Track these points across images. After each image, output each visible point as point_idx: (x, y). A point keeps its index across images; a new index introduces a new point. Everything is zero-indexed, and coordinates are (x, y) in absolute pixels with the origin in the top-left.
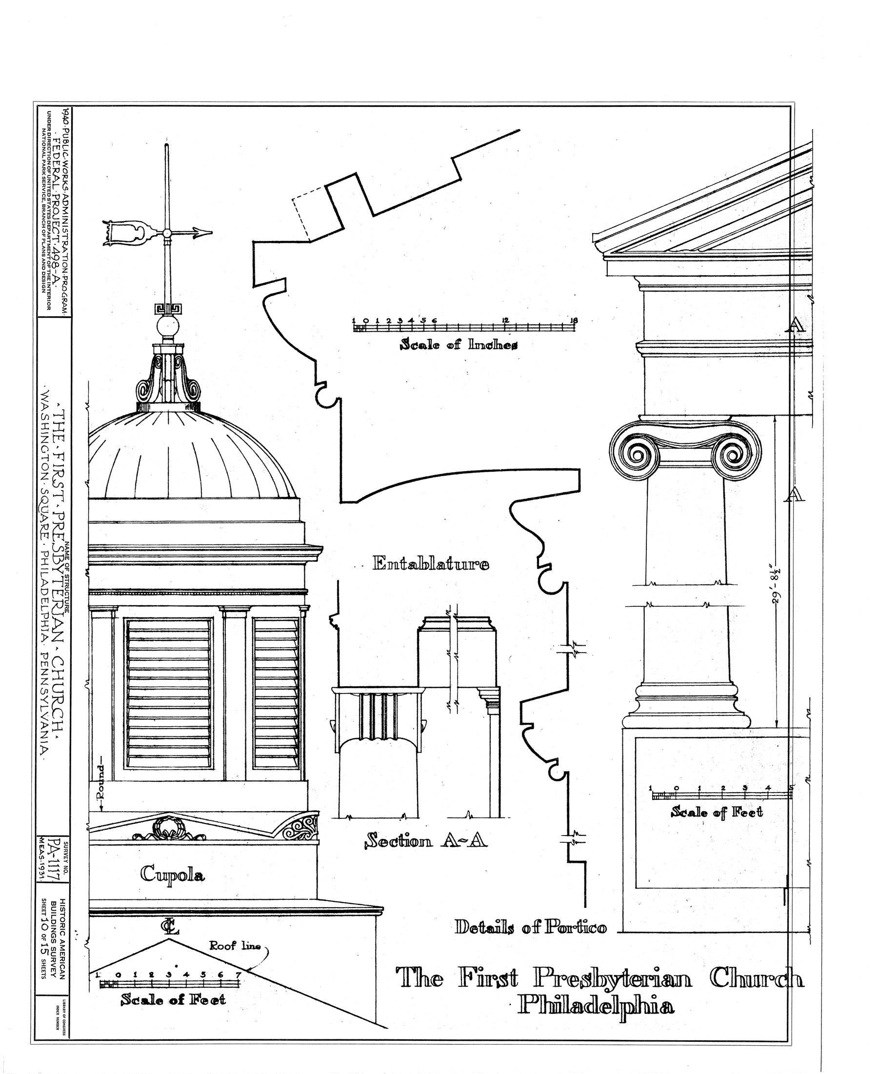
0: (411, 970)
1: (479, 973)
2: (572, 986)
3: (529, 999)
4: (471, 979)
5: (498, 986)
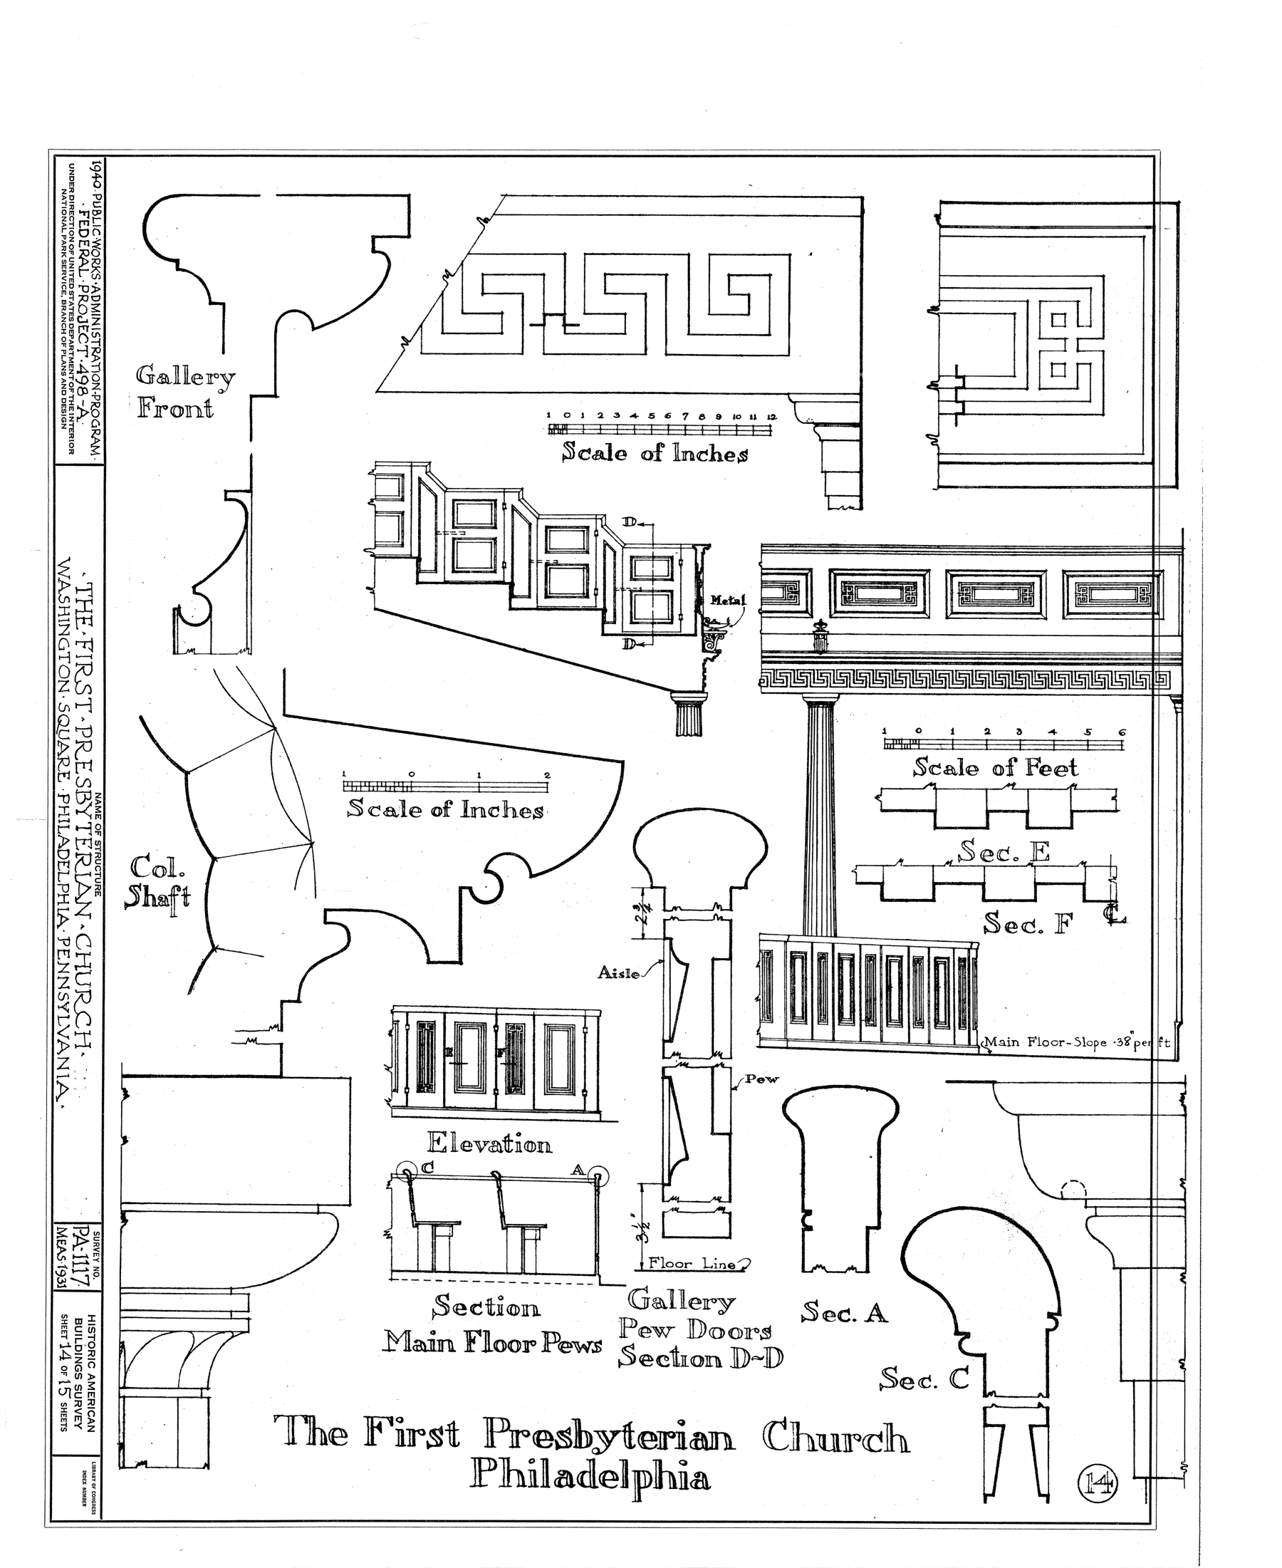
0: (299, 1421)
2: (539, 1446)
3: (485, 1465)
5: (429, 1446)
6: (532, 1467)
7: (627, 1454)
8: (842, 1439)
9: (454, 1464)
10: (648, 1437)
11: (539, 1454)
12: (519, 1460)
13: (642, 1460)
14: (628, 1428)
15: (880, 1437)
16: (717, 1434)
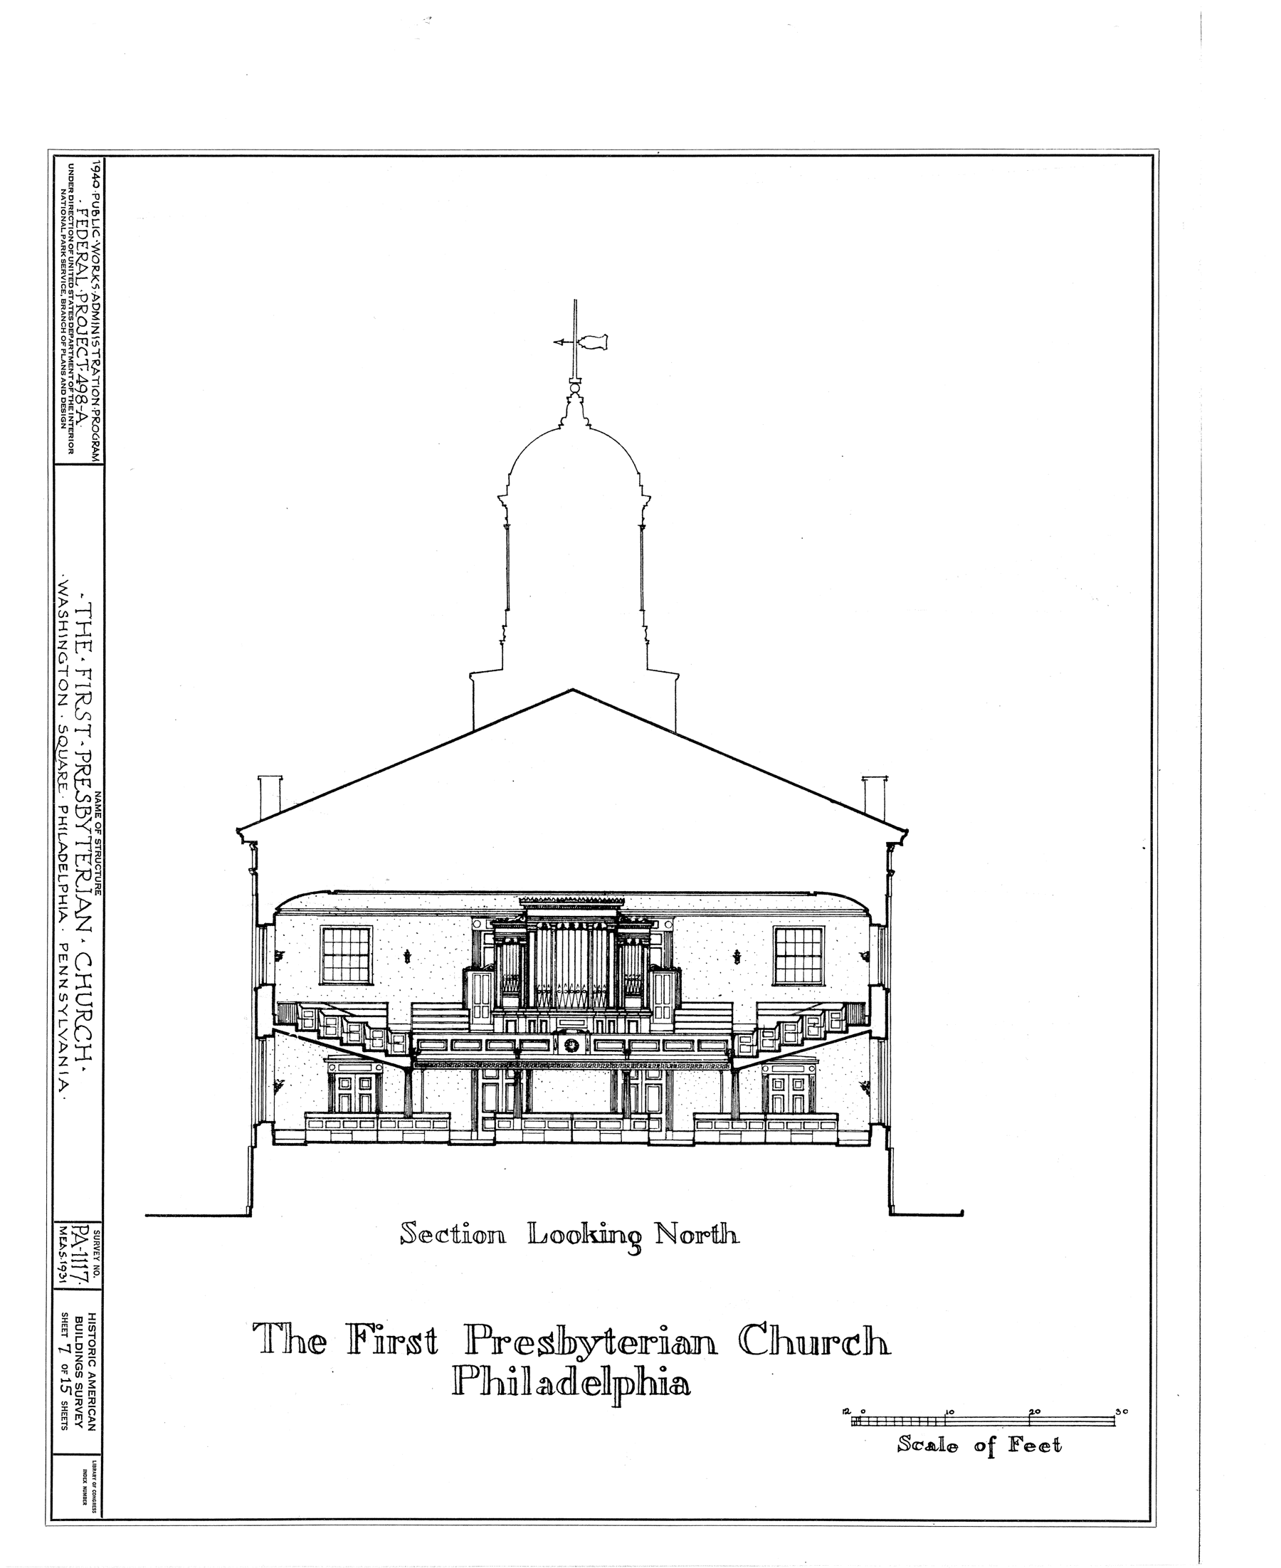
1: (378, 1333)
2: (521, 1353)
3: (467, 1372)
4: (364, 1340)
5: (409, 1352)
6: (513, 1375)
7: (608, 1359)
8: (820, 1342)
9: (433, 1371)
10: (628, 1342)
11: (520, 1361)
12: (500, 1369)
13: (624, 1366)
14: (609, 1335)
15: (857, 1338)
16: (700, 1339)
